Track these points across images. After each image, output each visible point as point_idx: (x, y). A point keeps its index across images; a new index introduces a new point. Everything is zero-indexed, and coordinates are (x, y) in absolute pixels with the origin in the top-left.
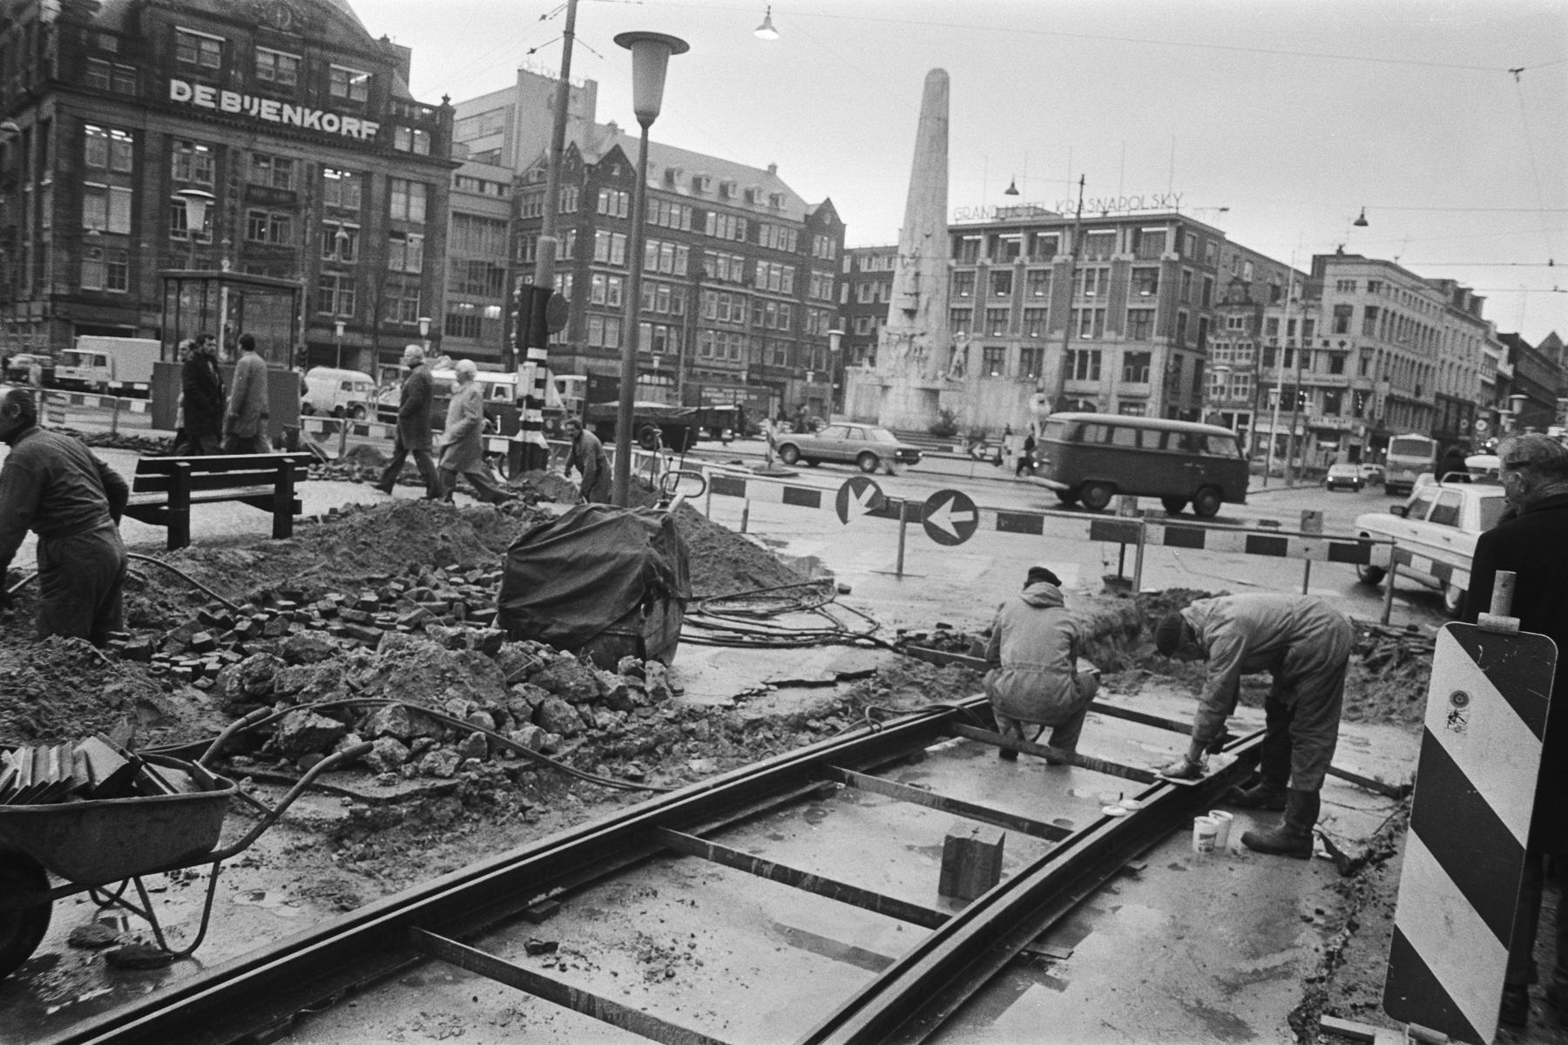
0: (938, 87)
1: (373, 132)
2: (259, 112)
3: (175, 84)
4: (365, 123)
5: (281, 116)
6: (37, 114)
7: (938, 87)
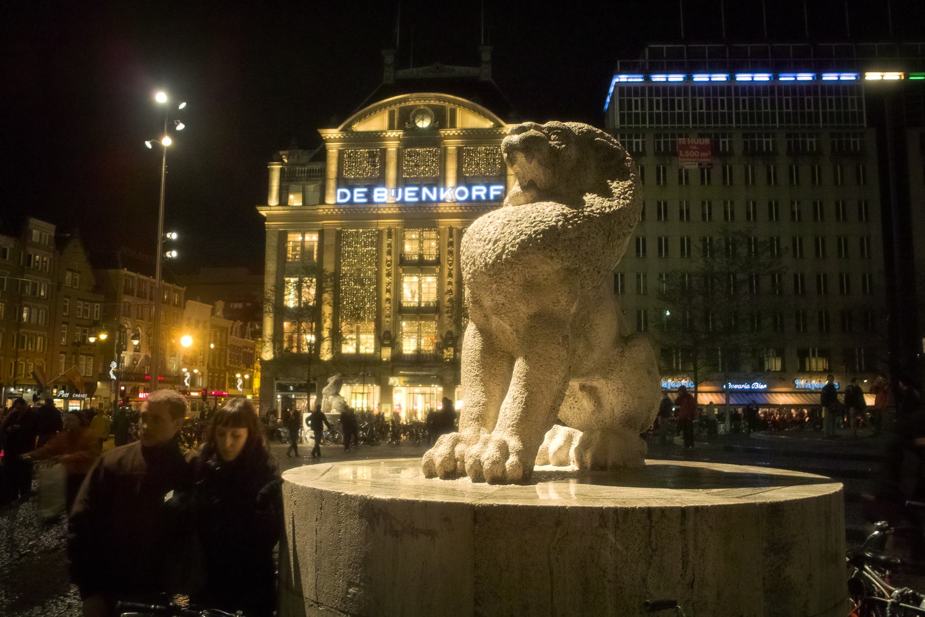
1: (498, 193)
5: (420, 198)
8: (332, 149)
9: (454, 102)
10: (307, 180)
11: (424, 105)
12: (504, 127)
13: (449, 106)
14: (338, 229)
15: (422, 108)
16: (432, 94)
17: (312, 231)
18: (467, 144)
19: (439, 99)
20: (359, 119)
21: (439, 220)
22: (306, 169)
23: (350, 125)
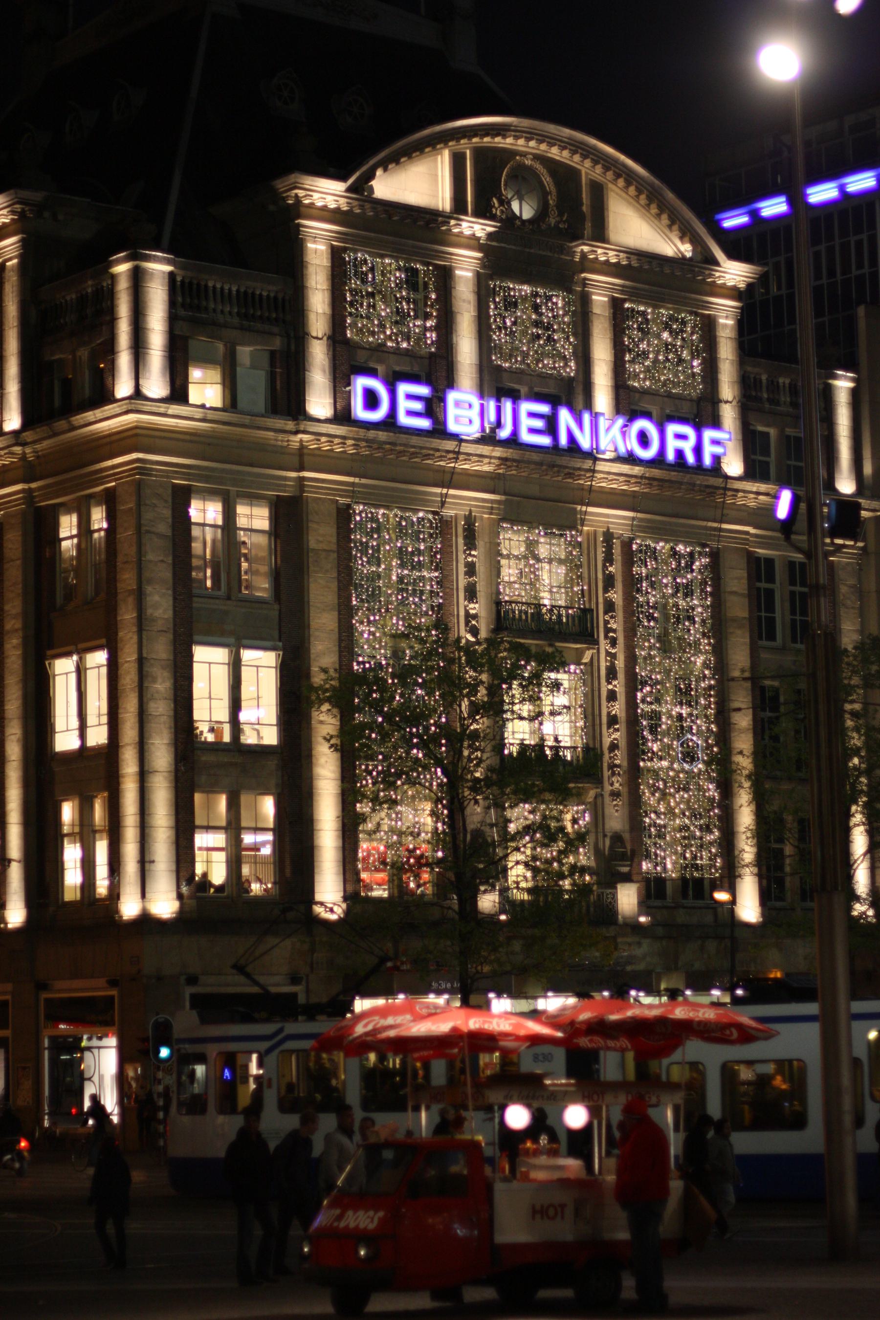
2: (515, 432)
4: (709, 434)
8: (315, 238)
9: (609, 164)
10: (242, 328)
11: (537, 157)
12: (718, 264)
13: (587, 170)
14: (342, 500)
15: (528, 162)
16: (567, 132)
17: (252, 498)
18: (635, 295)
19: (576, 147)
20: (385, 165)
21: (591, 509)
22: (234, 289)
23: (370, 175)
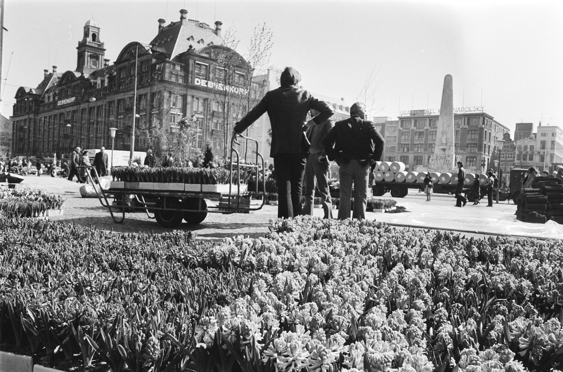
0: (448, 81)
3: (196, 79)
6: (150, 90)
7: (448, 81)
